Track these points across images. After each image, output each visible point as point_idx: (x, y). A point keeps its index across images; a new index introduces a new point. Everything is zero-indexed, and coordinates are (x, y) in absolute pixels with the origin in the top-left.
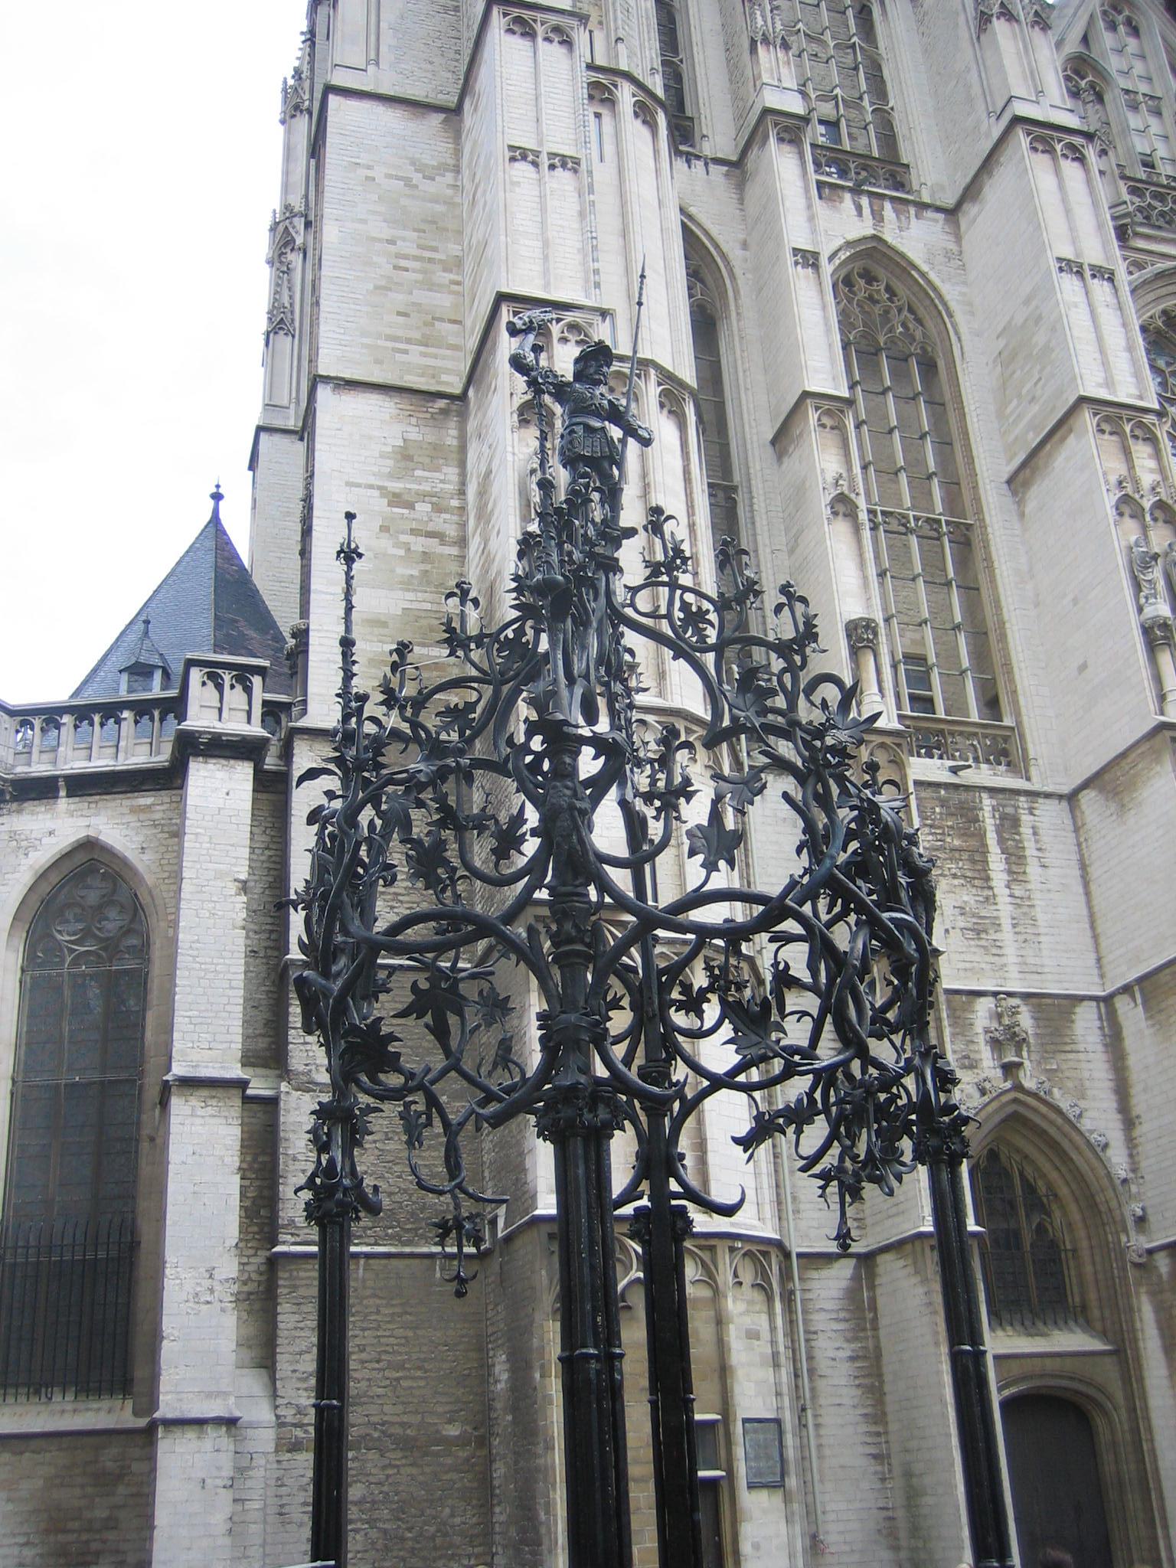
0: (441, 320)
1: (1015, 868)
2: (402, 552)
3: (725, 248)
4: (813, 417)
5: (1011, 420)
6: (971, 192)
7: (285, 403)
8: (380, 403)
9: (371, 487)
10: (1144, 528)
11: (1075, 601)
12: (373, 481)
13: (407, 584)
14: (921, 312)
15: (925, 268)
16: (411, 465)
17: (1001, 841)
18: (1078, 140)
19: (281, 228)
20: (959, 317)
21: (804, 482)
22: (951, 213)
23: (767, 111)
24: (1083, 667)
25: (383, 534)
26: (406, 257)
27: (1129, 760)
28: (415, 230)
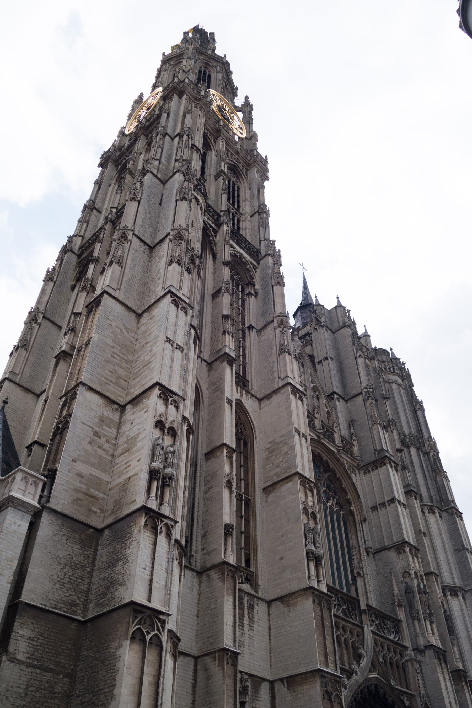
0: (122, 379)
1: (251, 624)
2: (94, 453)
3: (202, 388)
4: (225, 452)
5: (268, 470)
6: (268, 397)
7: (17, 373)
8: (98, 399)
9: (89, 426)
10: (308, 519)
11: (282, 536)
12: (90, 424)
14: (246, 426)
15: (251, 414)
16: (103, 423)
17: (249, 613)
18: (302, 395)
19: (33, 314)
20: (257, 433)
21: (216, 472)
23: (226, 353)
24: (282, 559)
25: (89, 445)
26: (116, 354)
27: (295, 596)
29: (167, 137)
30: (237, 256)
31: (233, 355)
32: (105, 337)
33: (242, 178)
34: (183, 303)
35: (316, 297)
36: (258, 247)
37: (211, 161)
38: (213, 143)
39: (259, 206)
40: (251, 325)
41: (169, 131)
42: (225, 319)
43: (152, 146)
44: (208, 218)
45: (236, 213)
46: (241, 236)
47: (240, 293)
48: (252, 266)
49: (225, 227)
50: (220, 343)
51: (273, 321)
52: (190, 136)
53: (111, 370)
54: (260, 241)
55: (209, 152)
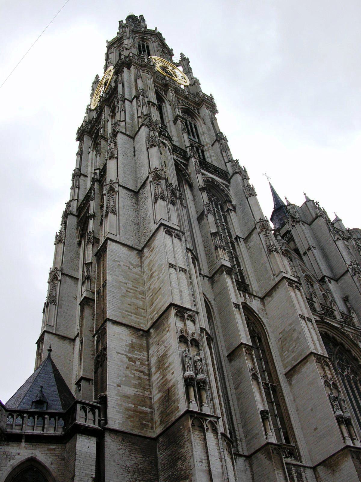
0: (140, 308)
3: (210, 300)
4: (244, 350)
5: (285, 357)
6: (269, 294)
7: (52, 325)
10: (331, 390)
11: (312, 410)
12: (124, 352)
13: (135, 386)
14: (257, 325)
15: (258, 313)
16: (134, 349)
18: (298, 285)
19: (53, 273)
20: (267, 327)
21: (241, 368)
22: (262, 299)
23: (223, 265)
24: (316, 429)
25: (127, 370)
26: (130, 289)
28: (131, 281)
29: (126, 101)
30: (209, 181)
31: (229, 265)
32: (117, 276)
33: (197, 118)
35: (286, 198)
36: (224, 169)
37: (167, 110)
39: (217, 135)
40: (237, 236)
41: (127, 96)
42: (213, 236)
43: (116, 112)
44: (177, 156)
45: (199, 146)
46: (208, 163)
47: (221, 212)
48: (224, 186)
49: (193, 160)
50: (215, 257)
51: (255, 228)
52: (145, 96)
53: (129, 303)
54: (226, 163)
55: (163, 104)
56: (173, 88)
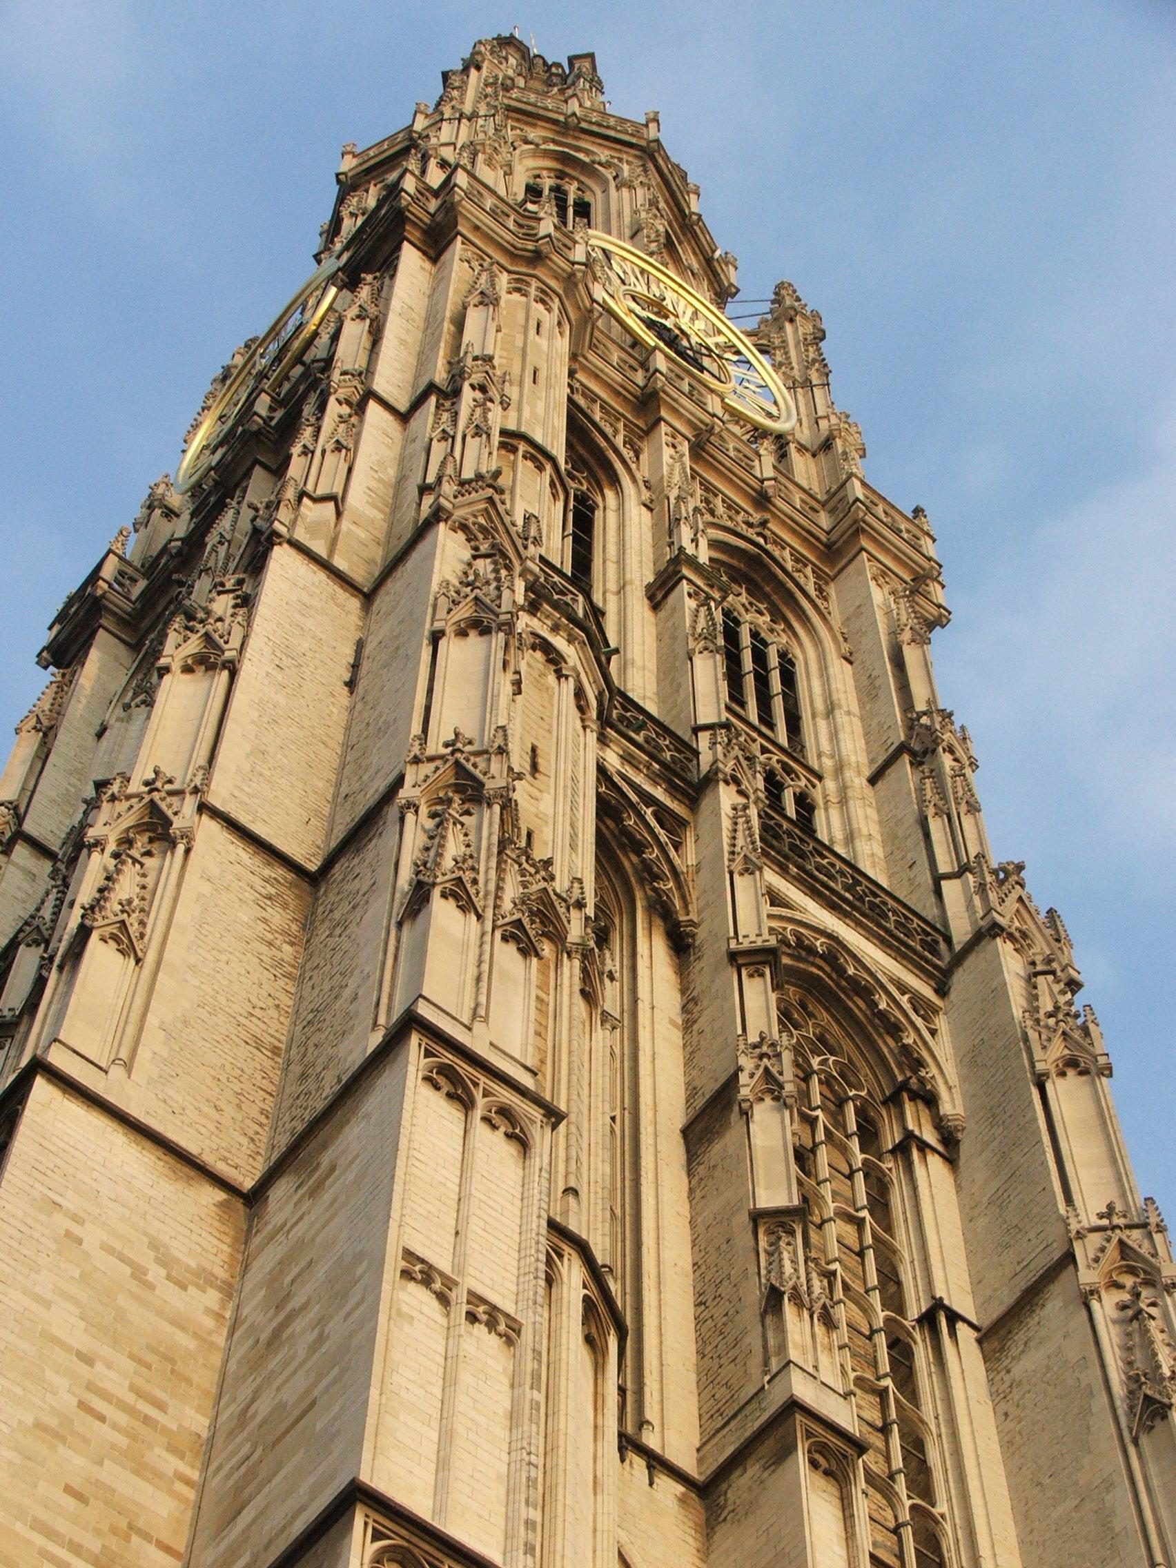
0: (147, 1537)
23: (793, 1406)
28: (132, 1357)
29: (373, 407)
30: (811, 950)
31: (844, 1415)
32: (39, 1299)
34: (495, 1087)
36: (931, 913)
37: (621, 527)
38: (627, 454)
39: (911, 724)
40: (938, 1305)
41: (381, 385)
42: (770, 1232)
43: (296, 450)
44: (626, 758)
45: (788, 770)
46: (825, 849)
47: (855, 1144)
48: (904, 1000)
49: (727, 797)
50: (757, 1358)
51: (1069, 1258)
52: (494, 392)
53: (76, 1484)
54: (938, 879)
55: (609, 494)
56: (690, 423)
